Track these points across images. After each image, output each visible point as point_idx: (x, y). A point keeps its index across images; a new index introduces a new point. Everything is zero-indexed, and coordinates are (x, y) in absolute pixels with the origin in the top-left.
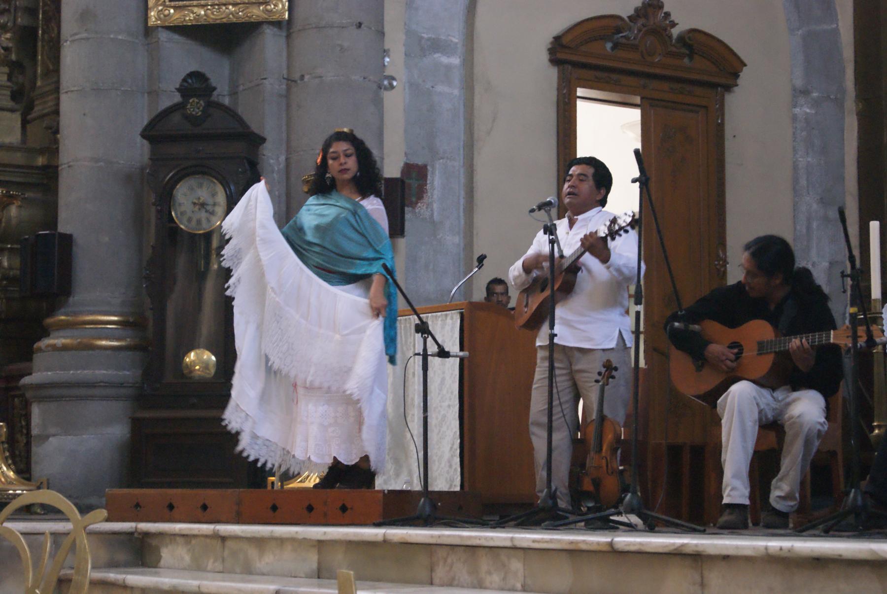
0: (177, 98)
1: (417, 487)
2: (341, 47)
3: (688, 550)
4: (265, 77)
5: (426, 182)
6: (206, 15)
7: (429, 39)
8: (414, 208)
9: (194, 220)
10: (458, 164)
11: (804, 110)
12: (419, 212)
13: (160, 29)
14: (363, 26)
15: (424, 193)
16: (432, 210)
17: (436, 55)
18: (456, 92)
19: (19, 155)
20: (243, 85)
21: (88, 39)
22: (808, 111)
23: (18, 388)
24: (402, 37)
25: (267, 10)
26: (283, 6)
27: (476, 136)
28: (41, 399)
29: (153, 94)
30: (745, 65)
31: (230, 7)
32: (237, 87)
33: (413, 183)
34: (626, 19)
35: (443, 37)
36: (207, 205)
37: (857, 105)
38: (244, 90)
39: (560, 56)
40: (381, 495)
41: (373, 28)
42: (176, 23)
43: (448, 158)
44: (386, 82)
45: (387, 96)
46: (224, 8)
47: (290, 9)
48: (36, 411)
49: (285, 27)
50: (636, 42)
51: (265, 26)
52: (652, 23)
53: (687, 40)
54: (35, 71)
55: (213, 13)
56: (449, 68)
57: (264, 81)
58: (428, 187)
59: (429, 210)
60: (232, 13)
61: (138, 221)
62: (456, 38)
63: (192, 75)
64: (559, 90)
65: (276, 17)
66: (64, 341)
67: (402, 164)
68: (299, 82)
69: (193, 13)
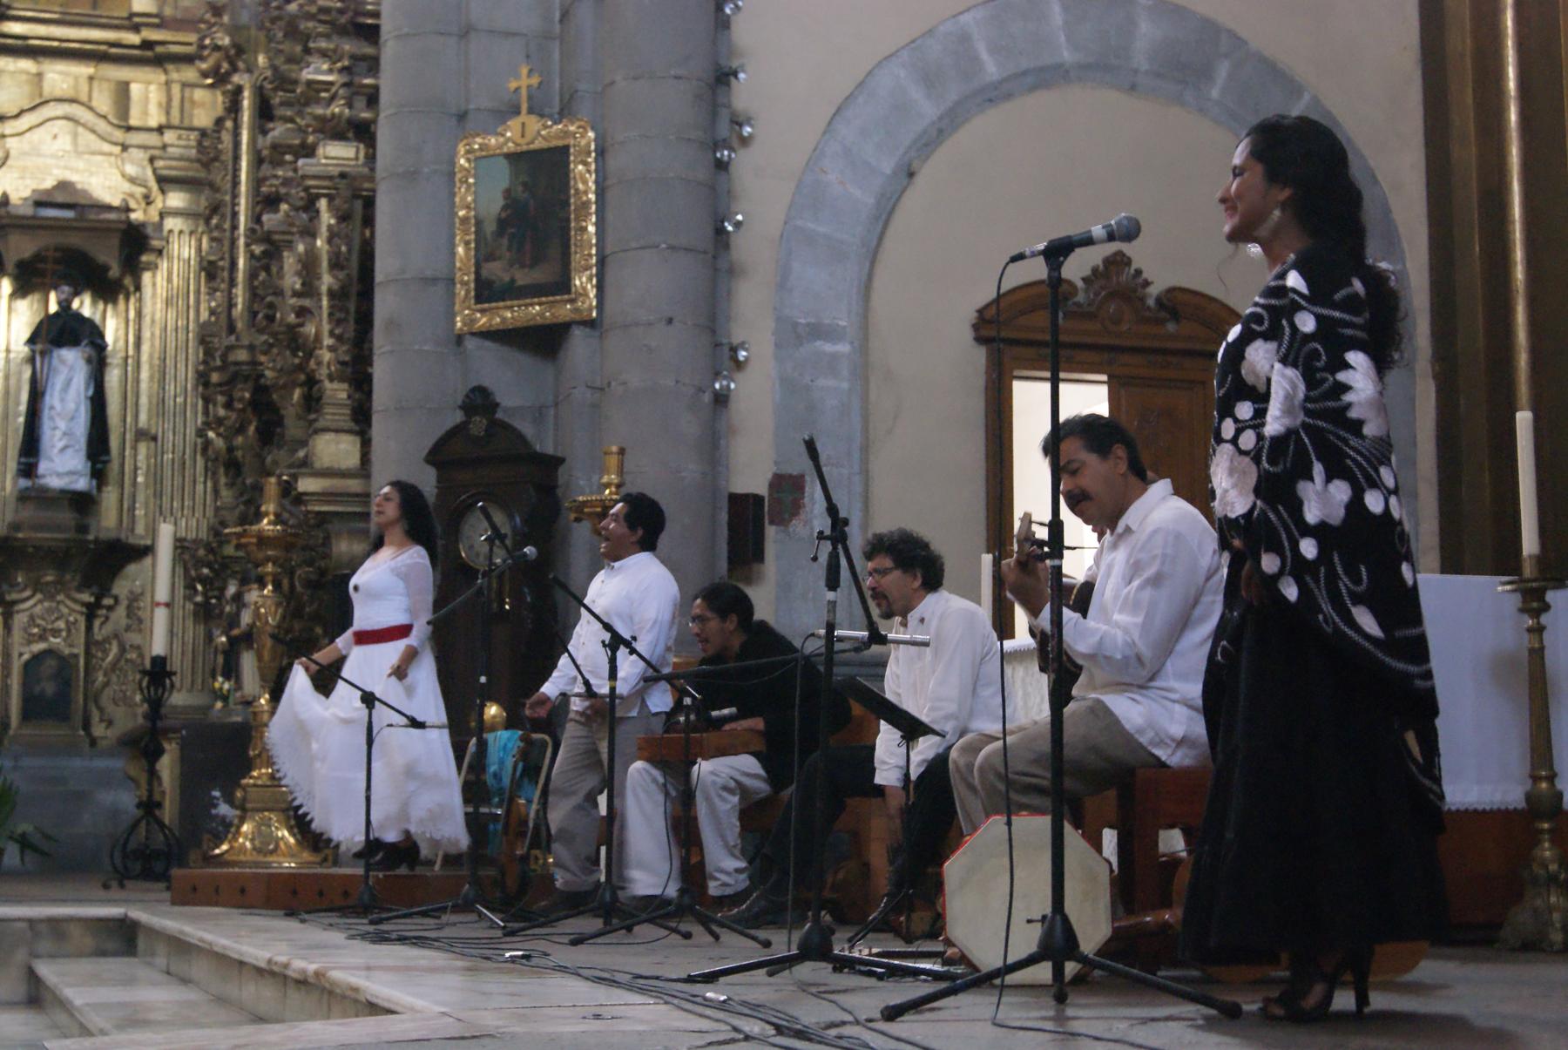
5: (803, 493)
6: (512, 318)
7: (808, 325)
8: (786, 526)
12: (794, 531)
13: (468, 336)
17: (818, 343)
35: (827, 321)
39: (985, 333)
50: (1092, 309)
56: (834, 357)
57: (574, 391)
58: (806, 500)
67: (769, 476)
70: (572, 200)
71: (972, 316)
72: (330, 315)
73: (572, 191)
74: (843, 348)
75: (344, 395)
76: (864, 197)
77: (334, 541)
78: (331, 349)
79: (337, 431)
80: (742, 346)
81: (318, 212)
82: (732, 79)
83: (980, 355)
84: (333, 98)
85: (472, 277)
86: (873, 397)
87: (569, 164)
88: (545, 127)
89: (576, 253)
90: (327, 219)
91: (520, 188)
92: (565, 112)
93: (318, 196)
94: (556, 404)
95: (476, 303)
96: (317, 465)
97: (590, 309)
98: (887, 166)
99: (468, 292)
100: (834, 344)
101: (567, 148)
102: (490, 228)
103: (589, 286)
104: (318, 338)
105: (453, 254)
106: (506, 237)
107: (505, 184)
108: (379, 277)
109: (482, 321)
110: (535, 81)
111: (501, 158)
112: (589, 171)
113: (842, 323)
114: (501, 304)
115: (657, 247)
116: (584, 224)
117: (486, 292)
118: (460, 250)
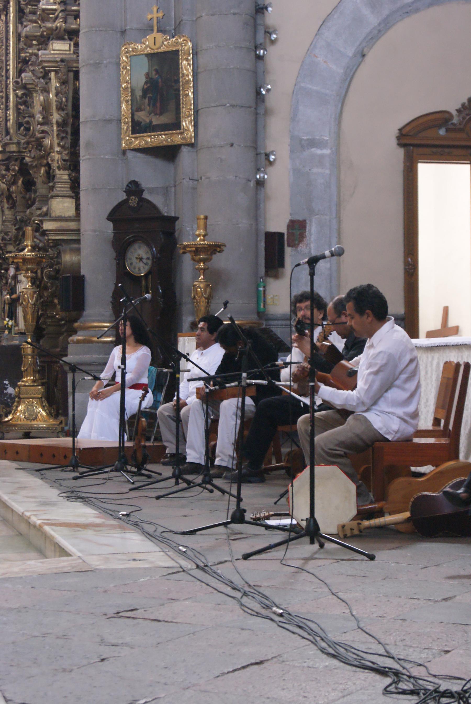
5: (305, 230)
6: (151, 142)
7: (308, 140)
8: (297, 247)
12: (301, 250)
13: (128, 151)
14: (234, 145)
16: (310, 248)
21: (89, 159)
24: (288, 140)
35: (317, 138)
41: (242, 145)
50: (462, 127)
51: (183, 147)
58: (307, 233)
59: (308, 248)
64: (405, 162)
67: (287, 221)
71: (394, 132)
72: (58, 135)
73: (181, 75)
74: (327, 152)
75: (66, 177)
77: (63, 256)
78: (59, 153)
79: (62, 196)
80: (272, 153)
81: (50, 79)
82: (265, 11)
83: (401, 152)
84: (56, 18)
85: (130, 120)
87: (179, 60)
88: (166, 40)
89: (183, 107)
90: (55, 83)
91: (154, 73)
92: (177, 32)
93: (50, 71)
94: (175, 186)
95: (132, 134)
96: (53, 215)
97: (191, 138)
98: (350, 52)
100: (321, 150)
101: (178, 51)
102: (139, 93)
103: (190, 126)
104: (52, 147)
106: (147, 99)
107: (146, 70)
108: (82, 119)
109: (137, 143)
110: (160, 15)
111: (144, 56)
112: (189, 64)
113: (326, 138)
114: (145, 134)
115: (225, 106)
116: (187, 92)
118: (124, 106)
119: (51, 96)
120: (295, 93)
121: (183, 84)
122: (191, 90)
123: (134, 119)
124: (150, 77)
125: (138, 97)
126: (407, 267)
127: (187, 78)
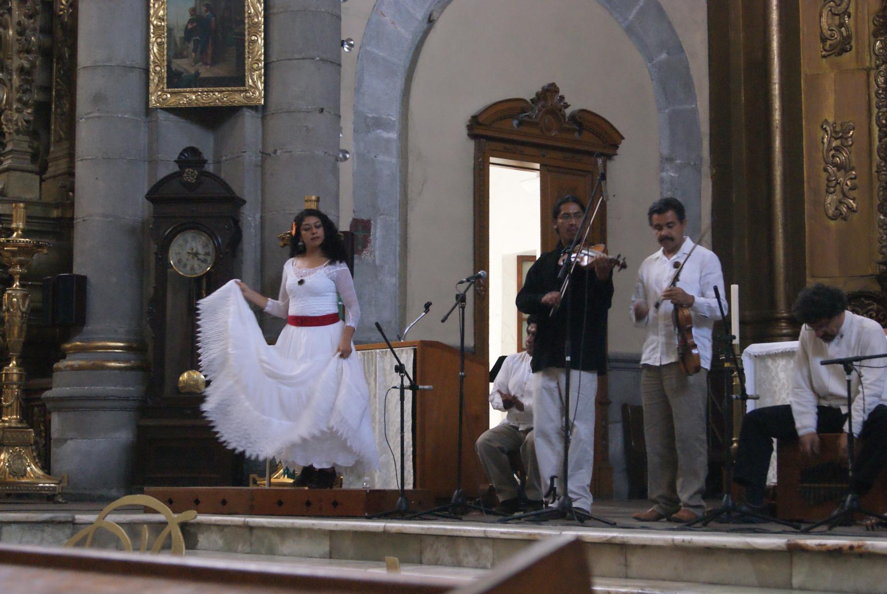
0: (176, 169)
1: (394, 485)
2: (308, 129)
3: (617, 541)
4: (244, 150)
5: (370, 233)
6: (196, 100)
7: (373, 118)
9: (188, 267)
10: (395, 219)
11: (670, 173)
13: (159, 110)
14: (324, 111)
15: (368, 242)
16: (374, 256)
17: (378, 131)
18: (394, 161)
19: (38, 208)
20: (226, 155)
21: (99, 117)
22: (673, 175)
23: (39, 399)
25: (247, 97)
26: (260, 94)
27: (409, 196)
28: (59, 410)
29: (153, 162)
30: (624, 139)
31: (217, 94)
32: (221, 157)
33: (360, 235)
34: (530, 101)
35: (384, 117)
36: (199, 254)
37: (711, 170)
38: (226, 160)
39: (477, 131)
40: (365, 493)
42: (172, 105)
43: (387, 215)
44: (341, 156)
45: (342, 165)
46: (211, 94)
47: (265, 97)
48: (56, 420)
49: (262, 110)
50: (537, 120)
51: (245, 109)
52: (550, 105)
53: (577, 117)
54: (49, 139)
55: (202, 98)
56: (388, 141)
59: (372, 256)
60: (218, 99)
61: (141, 265)
62: (394, 117)
63: (186, 150)
65: (254, 103)
66: (81, 363)
67: (351, 219)
68: (272, 155)
69: (186, 98)
70: (246, 21)
73: (247, 15)
76: (407, 35)
83: (471, 144)
85: (164, 70)
86: (410, 170)
89: (249, 57)
91: (204, 9)
95: (168, 87)
98: (420, 14)
99: (161, 80)
102: (179, 34)
105: (147, 50)
106: (192, 42)
107: (192, 5)
113: (393, 119)
114: (188, 89)
115: (313, 59)
117: (175, 80)
119: (11, 32)
120: (360, 57)
121: (249, 28)
122: (260, 36)
123: (171, 69)
124: (198, 13)
125: (178, 40)
126: (477, 288)
127: (256, 20)
